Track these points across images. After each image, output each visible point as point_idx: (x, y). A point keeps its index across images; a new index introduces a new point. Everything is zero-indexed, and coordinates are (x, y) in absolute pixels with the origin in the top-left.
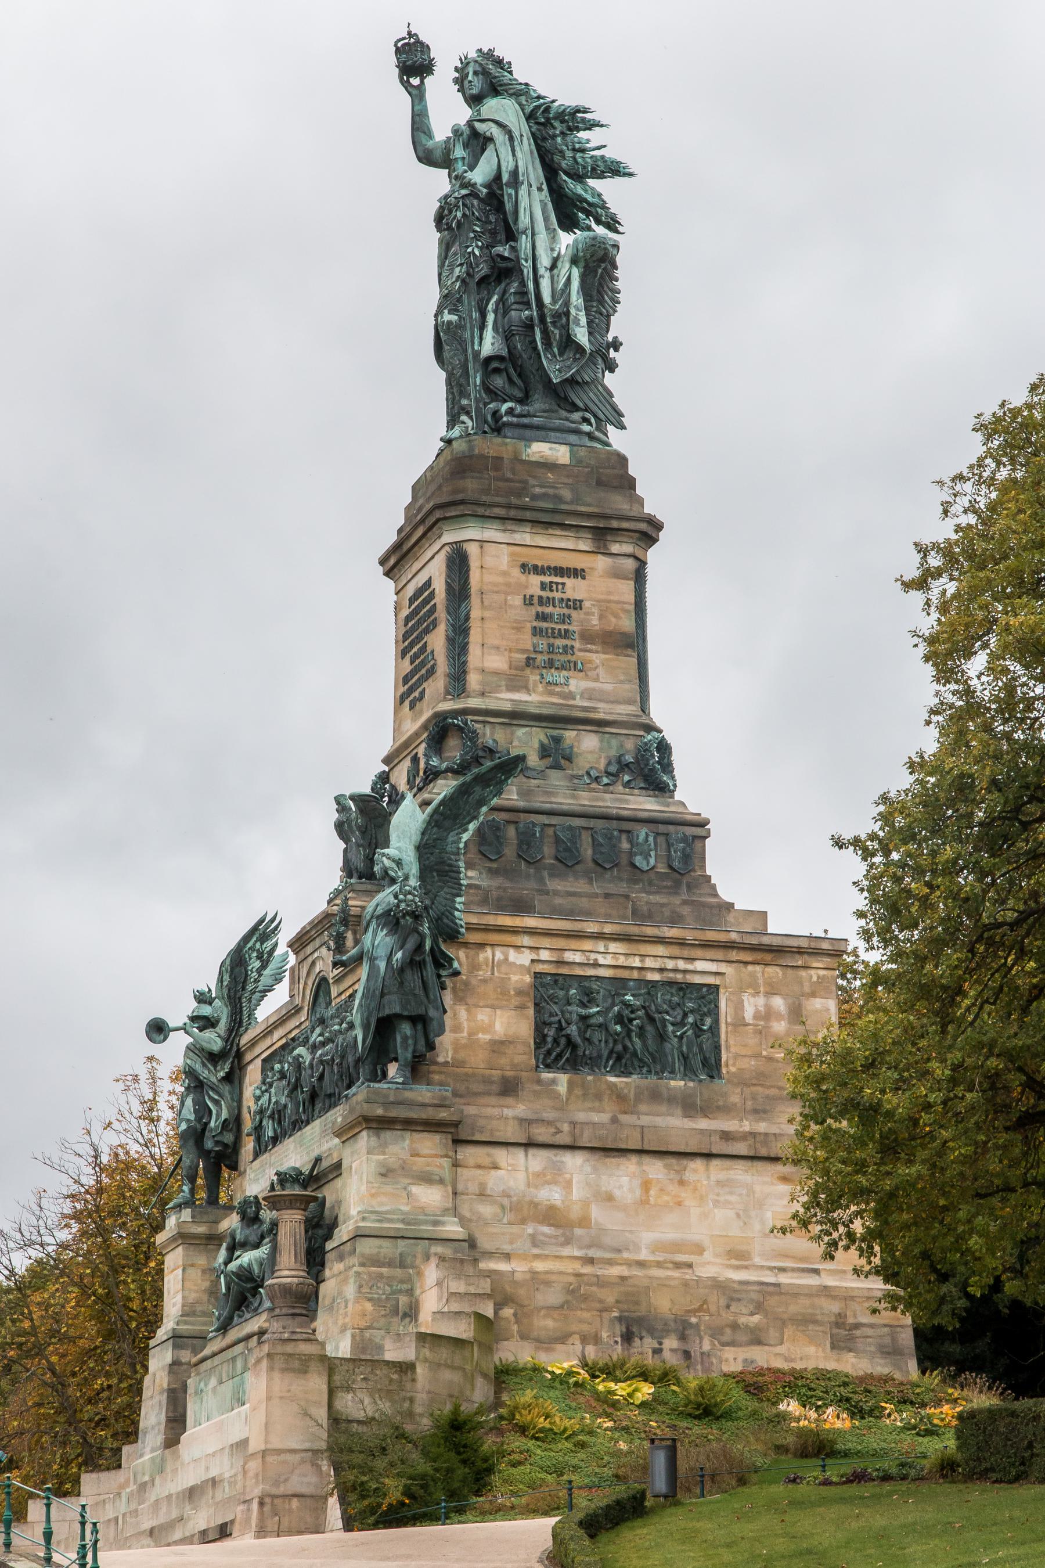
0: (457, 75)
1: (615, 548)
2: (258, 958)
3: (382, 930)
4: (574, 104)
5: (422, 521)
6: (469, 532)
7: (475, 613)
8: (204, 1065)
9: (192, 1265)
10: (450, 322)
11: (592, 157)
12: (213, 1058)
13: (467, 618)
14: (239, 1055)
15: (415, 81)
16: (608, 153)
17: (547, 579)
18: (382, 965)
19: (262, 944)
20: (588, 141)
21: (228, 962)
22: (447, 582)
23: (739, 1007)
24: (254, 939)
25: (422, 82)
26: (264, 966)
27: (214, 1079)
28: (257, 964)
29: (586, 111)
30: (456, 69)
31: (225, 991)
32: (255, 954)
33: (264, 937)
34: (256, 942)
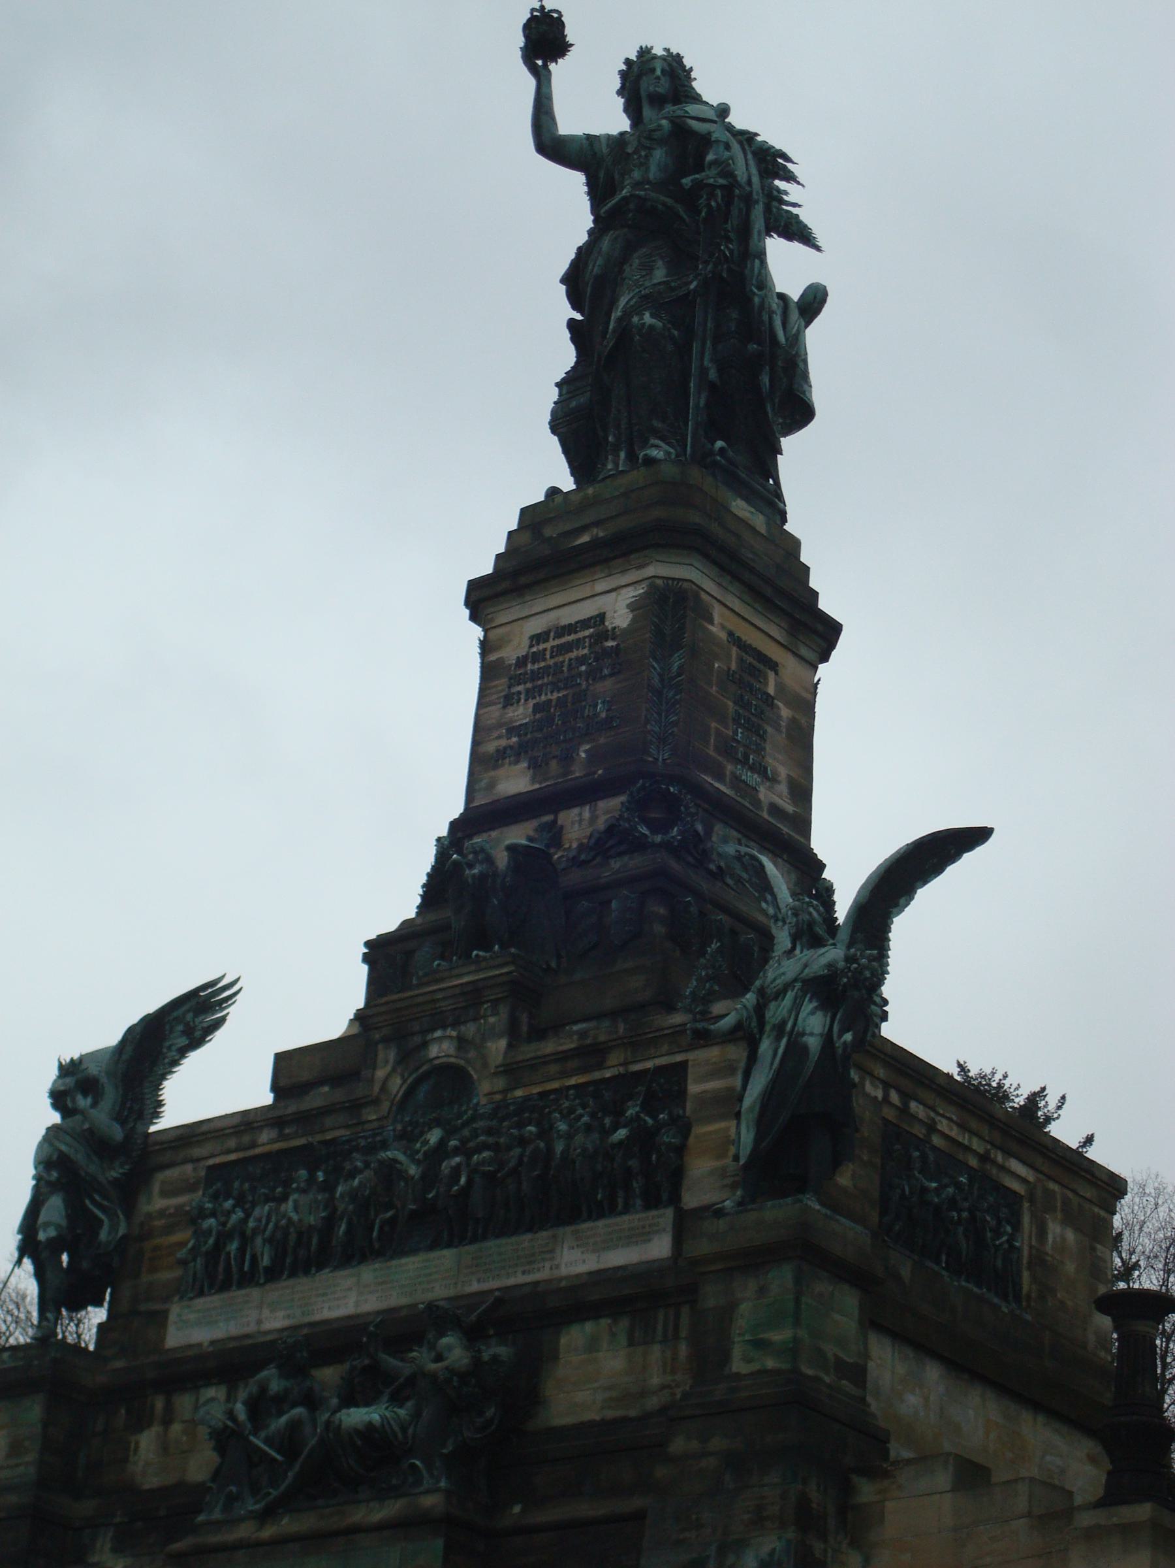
0: (624, 67)
1: (804, 651)
2: (184, 1033)
3: (810, 1001)
4: (778, 147)
10: (651, 327)
11: (787, 211)
15: (540, 62)
16: (805, 215)
17: (750, 660)
19: (196, 1016)
20: (786, 193)
23: (1042, 1233)
25: (545, 66)
29: (788, 160)
30: (628, 62)
32: (180, 1028)
34: (188, 1011)
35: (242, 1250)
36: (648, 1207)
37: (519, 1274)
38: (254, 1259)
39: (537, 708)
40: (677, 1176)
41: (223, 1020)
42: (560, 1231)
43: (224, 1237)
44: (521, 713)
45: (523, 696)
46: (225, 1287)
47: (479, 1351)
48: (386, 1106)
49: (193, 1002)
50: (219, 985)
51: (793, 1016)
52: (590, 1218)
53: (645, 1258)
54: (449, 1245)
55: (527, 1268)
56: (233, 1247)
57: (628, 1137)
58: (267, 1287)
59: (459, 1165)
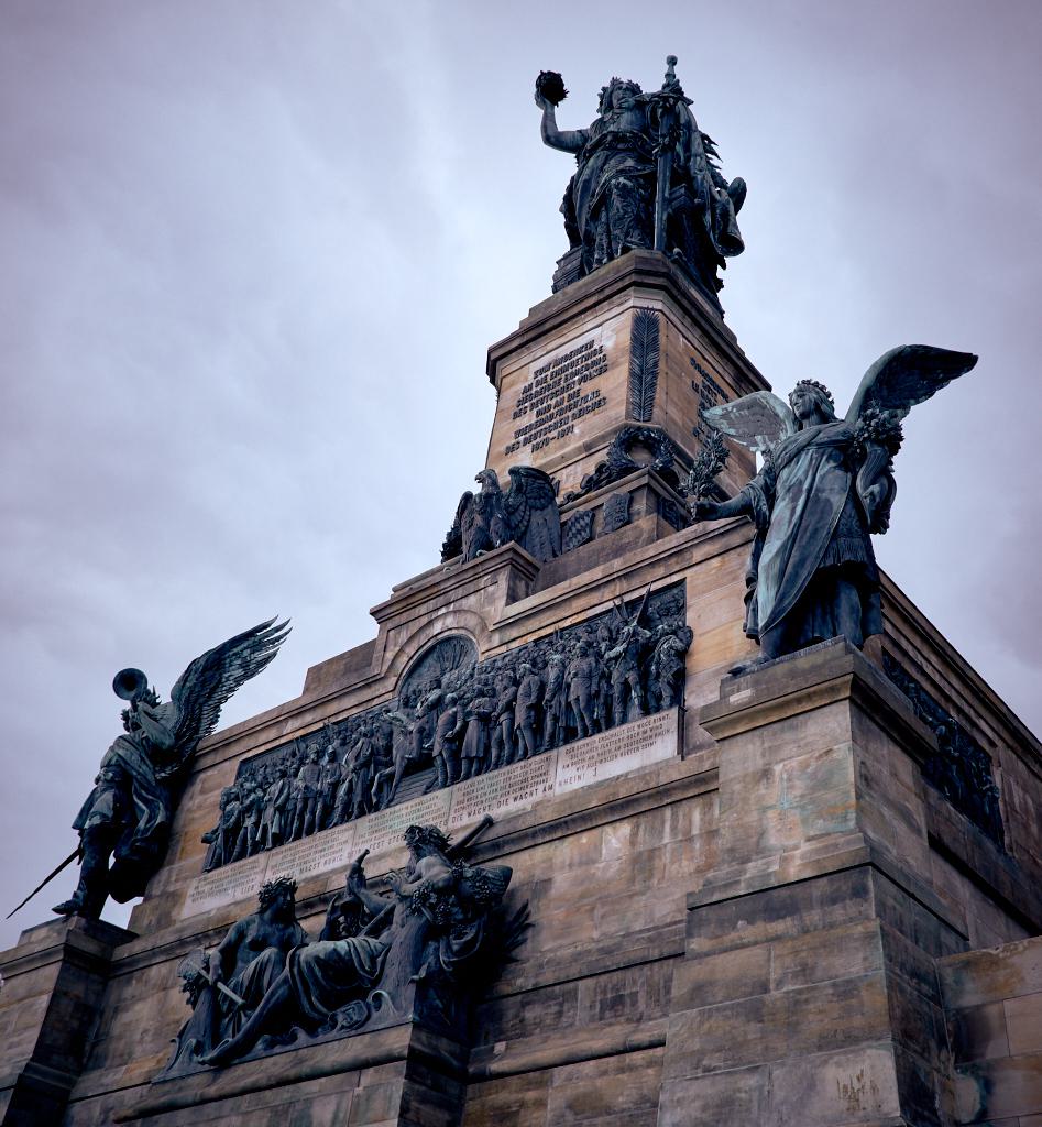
5: (600, 291)
6: (656, 303)
7: (662, 365)
8: (142, 759)
9: (66, 994)
12: (155, 753)
13: (656, 365)
14: (194, 758)
18: (838, 501)
21: (202, 662)
22: (633, 334)
24: (245, 645)
26: (249, 674)
27: (150, 777)
28: (240, 672)
31: (185, 693)
32: (239, 662)
33: (259, 646)
34: (246, 648)
35: (256, 824)
36: (647, 711)
37: (511, 801)
38: (265, 829)
39: (538, 414)
40: (680, 680)
41: (274, 654)
42: (554, 752)
43: (247, 810)
44: (530, 418)
45: (528, 409)
46: (242, 856)
47: (462, 867)
48: (393, 680)
49: (250, 641)
50: (272, 626)
51: (810, 473)
52: (586, 735)
53: (648, 762)
54: (444, 785)
55: (519, 794)
56: (249, 822)
57: (625, 651)
58: (274, 851)
59: (456, 713)
